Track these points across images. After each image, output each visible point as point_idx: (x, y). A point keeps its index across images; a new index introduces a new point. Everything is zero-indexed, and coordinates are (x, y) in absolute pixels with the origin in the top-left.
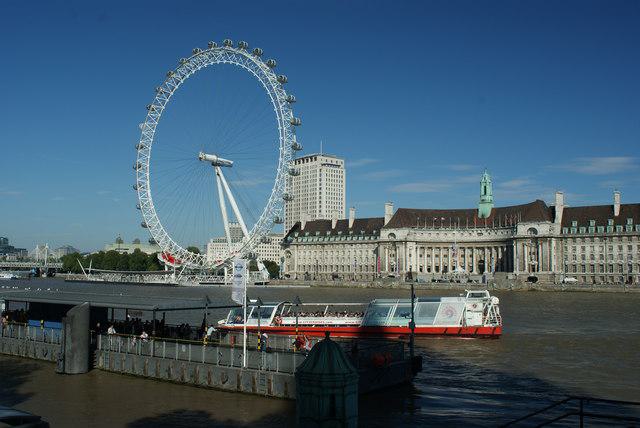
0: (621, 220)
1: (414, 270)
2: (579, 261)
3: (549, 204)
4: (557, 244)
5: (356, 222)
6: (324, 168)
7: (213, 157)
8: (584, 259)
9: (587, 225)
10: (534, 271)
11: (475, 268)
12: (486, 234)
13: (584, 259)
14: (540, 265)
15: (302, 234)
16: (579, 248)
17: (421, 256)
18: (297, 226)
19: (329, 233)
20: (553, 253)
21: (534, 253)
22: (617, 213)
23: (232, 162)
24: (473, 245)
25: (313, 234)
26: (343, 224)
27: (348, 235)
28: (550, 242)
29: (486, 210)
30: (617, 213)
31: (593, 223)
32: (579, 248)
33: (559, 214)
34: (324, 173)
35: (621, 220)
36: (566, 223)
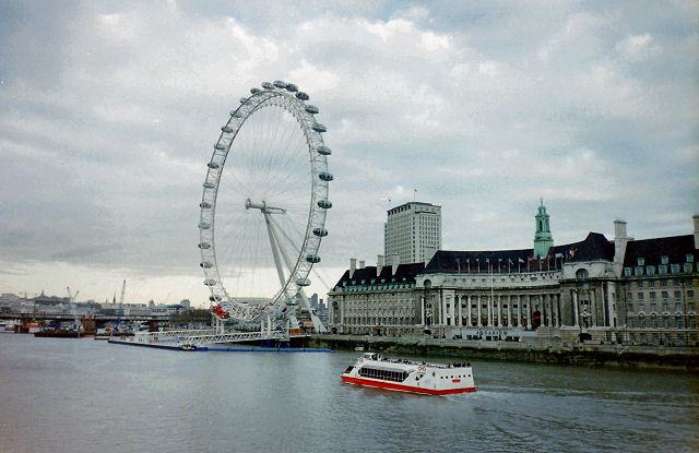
1: (453, 322)
3: (610, 237)
5: (400, 266)
12: (540, 278)
15: (349, 284)
16: (646, 293)
17: (464, 306)
18: (348, 272)
20: (611, 302)
21: (586, 302)
24: (528, 293)
25: (358, 284)
29: (542, 251)
31: (665, 260)
32: (646, 293)
33: (620, 252)
34: (417, 220)
36: (630, 261)
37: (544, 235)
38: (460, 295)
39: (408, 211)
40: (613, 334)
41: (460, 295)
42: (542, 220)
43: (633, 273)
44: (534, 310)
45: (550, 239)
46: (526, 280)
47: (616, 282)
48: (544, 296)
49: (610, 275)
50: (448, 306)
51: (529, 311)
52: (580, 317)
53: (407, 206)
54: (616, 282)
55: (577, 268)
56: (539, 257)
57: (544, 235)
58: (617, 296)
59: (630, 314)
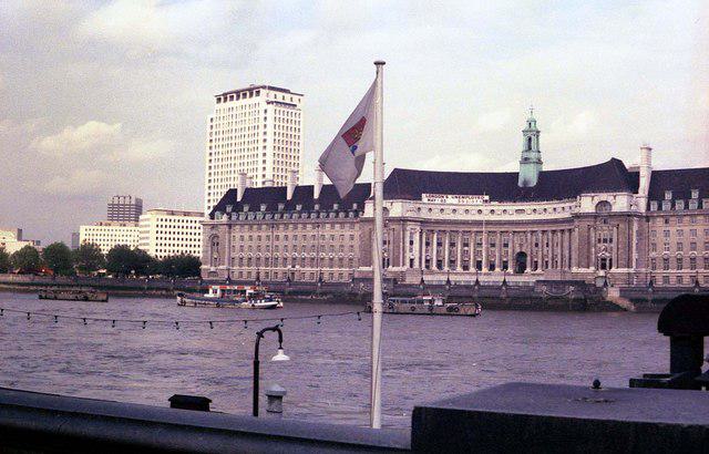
2: (673, 253)
3: (628, 164)
4: (640, 226)
6: (271, 108)
10: (603, 267)
11: (510, 264)
15: (238, 208)
17: (427, 244)
18: (232, 193)
19: (281, 207)
21: (605, 241)
26: (304, 193)
28: (630, 224)
29: (529, 175)
33: (644, 183)
34: (270, 115)
36: (654, 195)
37: (532, 155)
39: (255, 99)
42: (531, 136)
43: (660, 207)
44: (518, 250)
45: (539, 162)
50: (411, 243)
51: (510, 251)
52: (597, 257)
53: (253, 91)
55: (597, 200)
56: (525, 182)
57: (532, 155)
58: (639, 234)
59: (653, 254)
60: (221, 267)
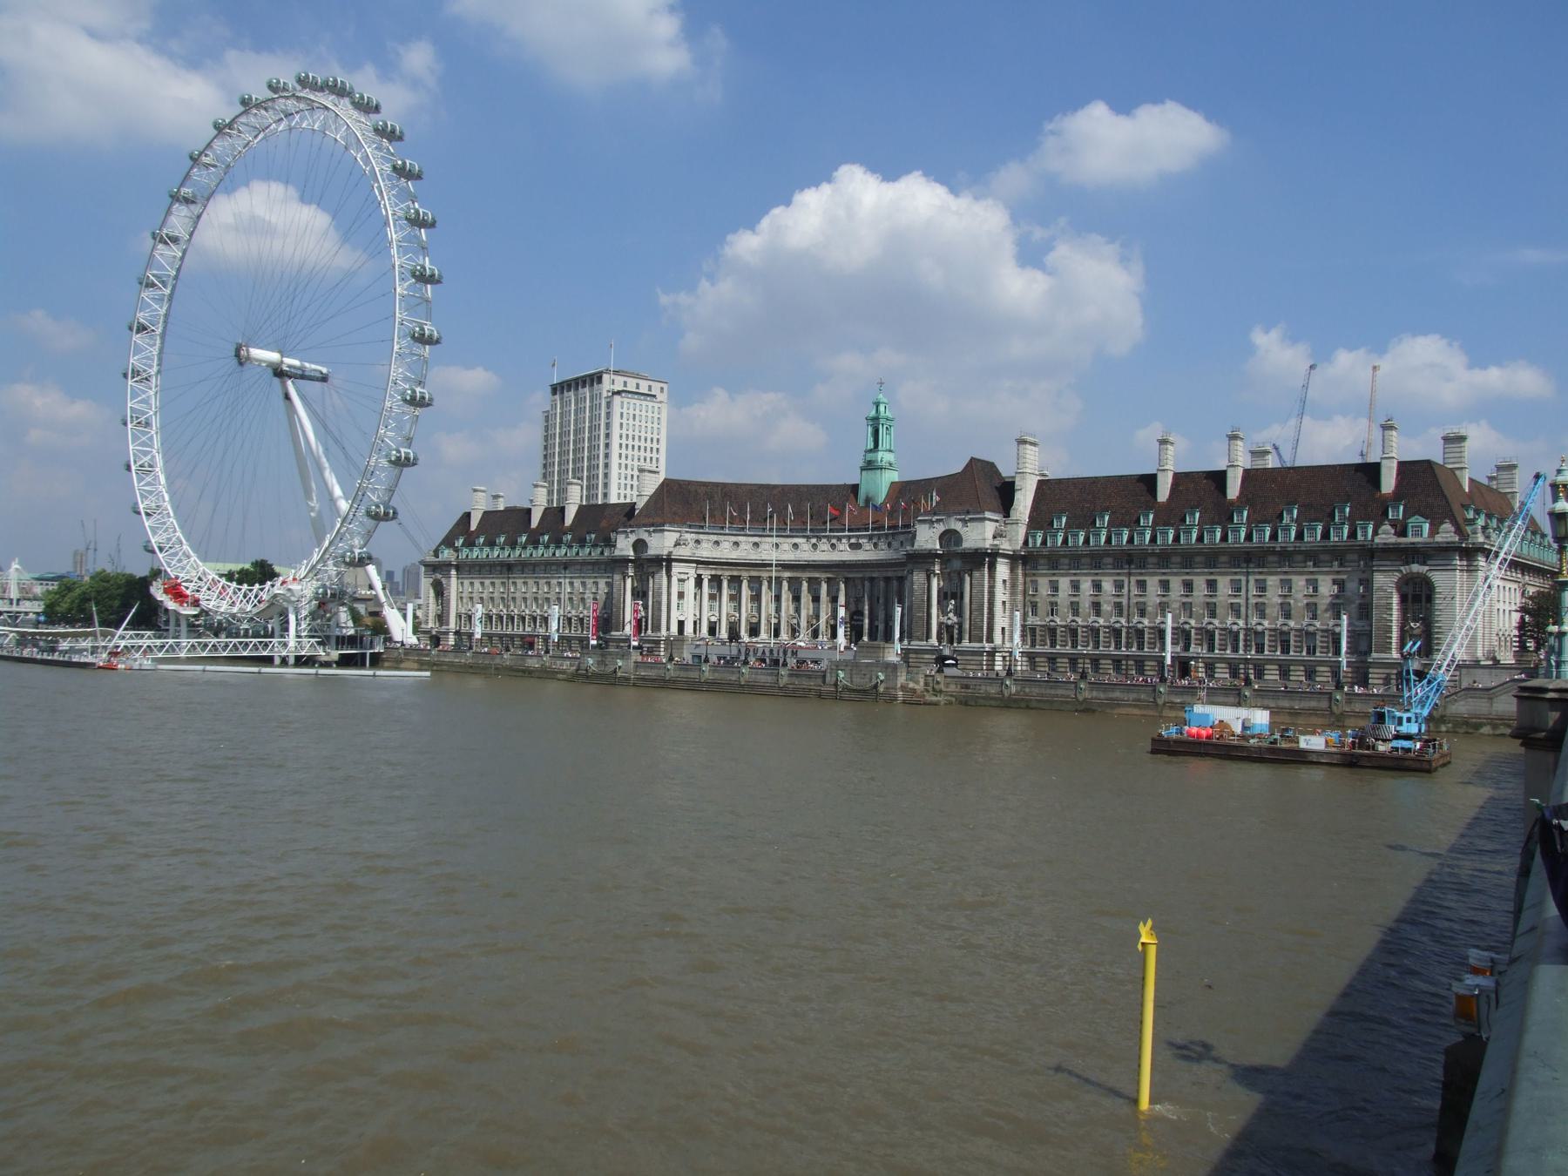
0: (1171, 515)
1: (689, 629)
3: (1006, 471)
4: (1013, 570)
6: (617, 399)
7: (274, 356)
8: (1076, 612)
9: (1089, 523)
12: (867, 545)
13: (1076, 612)
14: (967, 626)
15: (470, 544)
16: (1064, 583)
17: (712, 597)
20: (1001, 595)
21: (954, 596)
22: (1163, 494)
23: (324, 370)
27: (558, 542)
28: (992, 568)
30: (1163, 494)
33: (1024, 501)
35: (1171, 515)
36: (1040, 519)
38: (706, 574)
40: (998, 658)
41: (706, 574)
46: (841, 547)
47: (1014, 559)
48: (872, 579)
49: (1005, 546)
50: (681, 595)
52: (940, 625)
54: (1014, 559)
55: (941, 528)
56: (868, 500)
60: (444, 628)
